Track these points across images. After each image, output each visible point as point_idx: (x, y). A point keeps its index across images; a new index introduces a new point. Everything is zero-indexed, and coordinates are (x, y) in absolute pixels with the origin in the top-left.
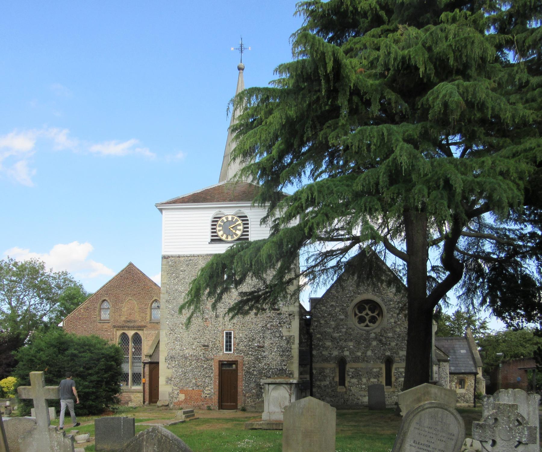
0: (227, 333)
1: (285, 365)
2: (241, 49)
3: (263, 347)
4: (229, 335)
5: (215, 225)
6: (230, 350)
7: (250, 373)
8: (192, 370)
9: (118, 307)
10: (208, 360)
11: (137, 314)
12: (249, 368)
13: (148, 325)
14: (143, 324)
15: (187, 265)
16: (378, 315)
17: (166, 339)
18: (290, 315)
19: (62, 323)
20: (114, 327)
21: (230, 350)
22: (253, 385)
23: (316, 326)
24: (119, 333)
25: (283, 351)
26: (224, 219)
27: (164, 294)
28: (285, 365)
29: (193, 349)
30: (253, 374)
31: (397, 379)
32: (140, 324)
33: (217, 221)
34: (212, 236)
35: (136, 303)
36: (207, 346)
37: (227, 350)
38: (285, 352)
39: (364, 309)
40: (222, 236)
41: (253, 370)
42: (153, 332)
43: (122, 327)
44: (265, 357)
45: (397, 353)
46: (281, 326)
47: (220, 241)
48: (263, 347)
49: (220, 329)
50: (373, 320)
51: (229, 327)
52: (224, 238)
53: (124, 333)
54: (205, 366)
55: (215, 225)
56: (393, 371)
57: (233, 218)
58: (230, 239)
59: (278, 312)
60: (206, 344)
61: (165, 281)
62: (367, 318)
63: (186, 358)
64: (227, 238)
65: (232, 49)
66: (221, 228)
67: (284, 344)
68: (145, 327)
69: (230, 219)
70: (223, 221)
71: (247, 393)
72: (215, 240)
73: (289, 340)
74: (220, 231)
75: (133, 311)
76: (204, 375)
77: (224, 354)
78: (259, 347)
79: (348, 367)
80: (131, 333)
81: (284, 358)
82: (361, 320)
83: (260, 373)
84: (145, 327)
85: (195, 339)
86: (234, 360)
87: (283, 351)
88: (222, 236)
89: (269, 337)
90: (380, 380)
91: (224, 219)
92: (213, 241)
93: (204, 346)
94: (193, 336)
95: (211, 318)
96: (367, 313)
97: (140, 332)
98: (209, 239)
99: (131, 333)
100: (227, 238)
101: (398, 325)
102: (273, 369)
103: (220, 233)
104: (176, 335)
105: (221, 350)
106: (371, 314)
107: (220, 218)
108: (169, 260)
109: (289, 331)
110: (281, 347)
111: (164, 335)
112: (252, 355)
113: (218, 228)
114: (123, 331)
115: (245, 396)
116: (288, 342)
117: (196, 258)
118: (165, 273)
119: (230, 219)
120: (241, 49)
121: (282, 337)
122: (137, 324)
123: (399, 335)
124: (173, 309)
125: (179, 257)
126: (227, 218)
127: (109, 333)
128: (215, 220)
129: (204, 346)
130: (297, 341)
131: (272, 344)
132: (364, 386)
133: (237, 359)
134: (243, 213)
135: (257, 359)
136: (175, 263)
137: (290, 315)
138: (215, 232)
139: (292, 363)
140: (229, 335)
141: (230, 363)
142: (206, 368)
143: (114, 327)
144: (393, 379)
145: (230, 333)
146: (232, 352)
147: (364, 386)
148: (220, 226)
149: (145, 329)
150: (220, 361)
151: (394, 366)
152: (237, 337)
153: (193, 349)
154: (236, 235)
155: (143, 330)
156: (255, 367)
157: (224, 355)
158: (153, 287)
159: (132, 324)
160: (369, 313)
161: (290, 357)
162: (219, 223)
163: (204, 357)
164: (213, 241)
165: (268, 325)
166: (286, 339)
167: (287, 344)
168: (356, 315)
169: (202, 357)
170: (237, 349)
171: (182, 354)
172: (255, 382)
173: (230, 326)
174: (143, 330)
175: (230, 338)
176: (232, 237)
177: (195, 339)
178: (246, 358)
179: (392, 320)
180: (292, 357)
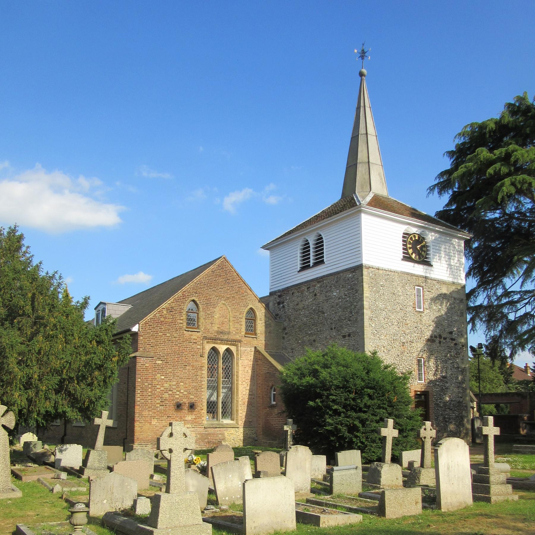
1: (461, 397)
2: (363, 55)
9: (209, 312)
12: (437, 400)
13: (244, 339)
14: (238, 337)
19: (137, 326)
20: (205, 338)
22: (441, 418)
24: (208, 347)
27: (367, 309)
28: (461, 397)
37: (419, 380)
40: (412, 254)
42: (249, 349)
43: (214, 340)
44: (447, 388)
46: (458, 357)
52: (413, 256)
53: (214, 349)
59: (454, 342)
65: (356, 51)
66: (411, 246)
68: (240, 341)
72: (407, 258)
74: (410, 248)
75: (226, 320)
80: (222, 348)
84: (240, 341)
97: (233, 348)
98: (401, 255)
99: (222, 348)
102: (454, 401)
103: (410, 251)
113: (408, 246)
114: (213, 345)
117: (393, 273)
120: (363, 55)
121: (458, 368)
122: (231, 337)
126: (415, 236)
127: (198, 347)
128: (406, 235)
136: (375, 275)
143: (205, 338)
146: (423, 382)
154: (423, 256)
156: (441, 399)
159: (225, 337)
166: (461, 371)
172: (442, 415)
174: (236, 345)
176: (420, 258)
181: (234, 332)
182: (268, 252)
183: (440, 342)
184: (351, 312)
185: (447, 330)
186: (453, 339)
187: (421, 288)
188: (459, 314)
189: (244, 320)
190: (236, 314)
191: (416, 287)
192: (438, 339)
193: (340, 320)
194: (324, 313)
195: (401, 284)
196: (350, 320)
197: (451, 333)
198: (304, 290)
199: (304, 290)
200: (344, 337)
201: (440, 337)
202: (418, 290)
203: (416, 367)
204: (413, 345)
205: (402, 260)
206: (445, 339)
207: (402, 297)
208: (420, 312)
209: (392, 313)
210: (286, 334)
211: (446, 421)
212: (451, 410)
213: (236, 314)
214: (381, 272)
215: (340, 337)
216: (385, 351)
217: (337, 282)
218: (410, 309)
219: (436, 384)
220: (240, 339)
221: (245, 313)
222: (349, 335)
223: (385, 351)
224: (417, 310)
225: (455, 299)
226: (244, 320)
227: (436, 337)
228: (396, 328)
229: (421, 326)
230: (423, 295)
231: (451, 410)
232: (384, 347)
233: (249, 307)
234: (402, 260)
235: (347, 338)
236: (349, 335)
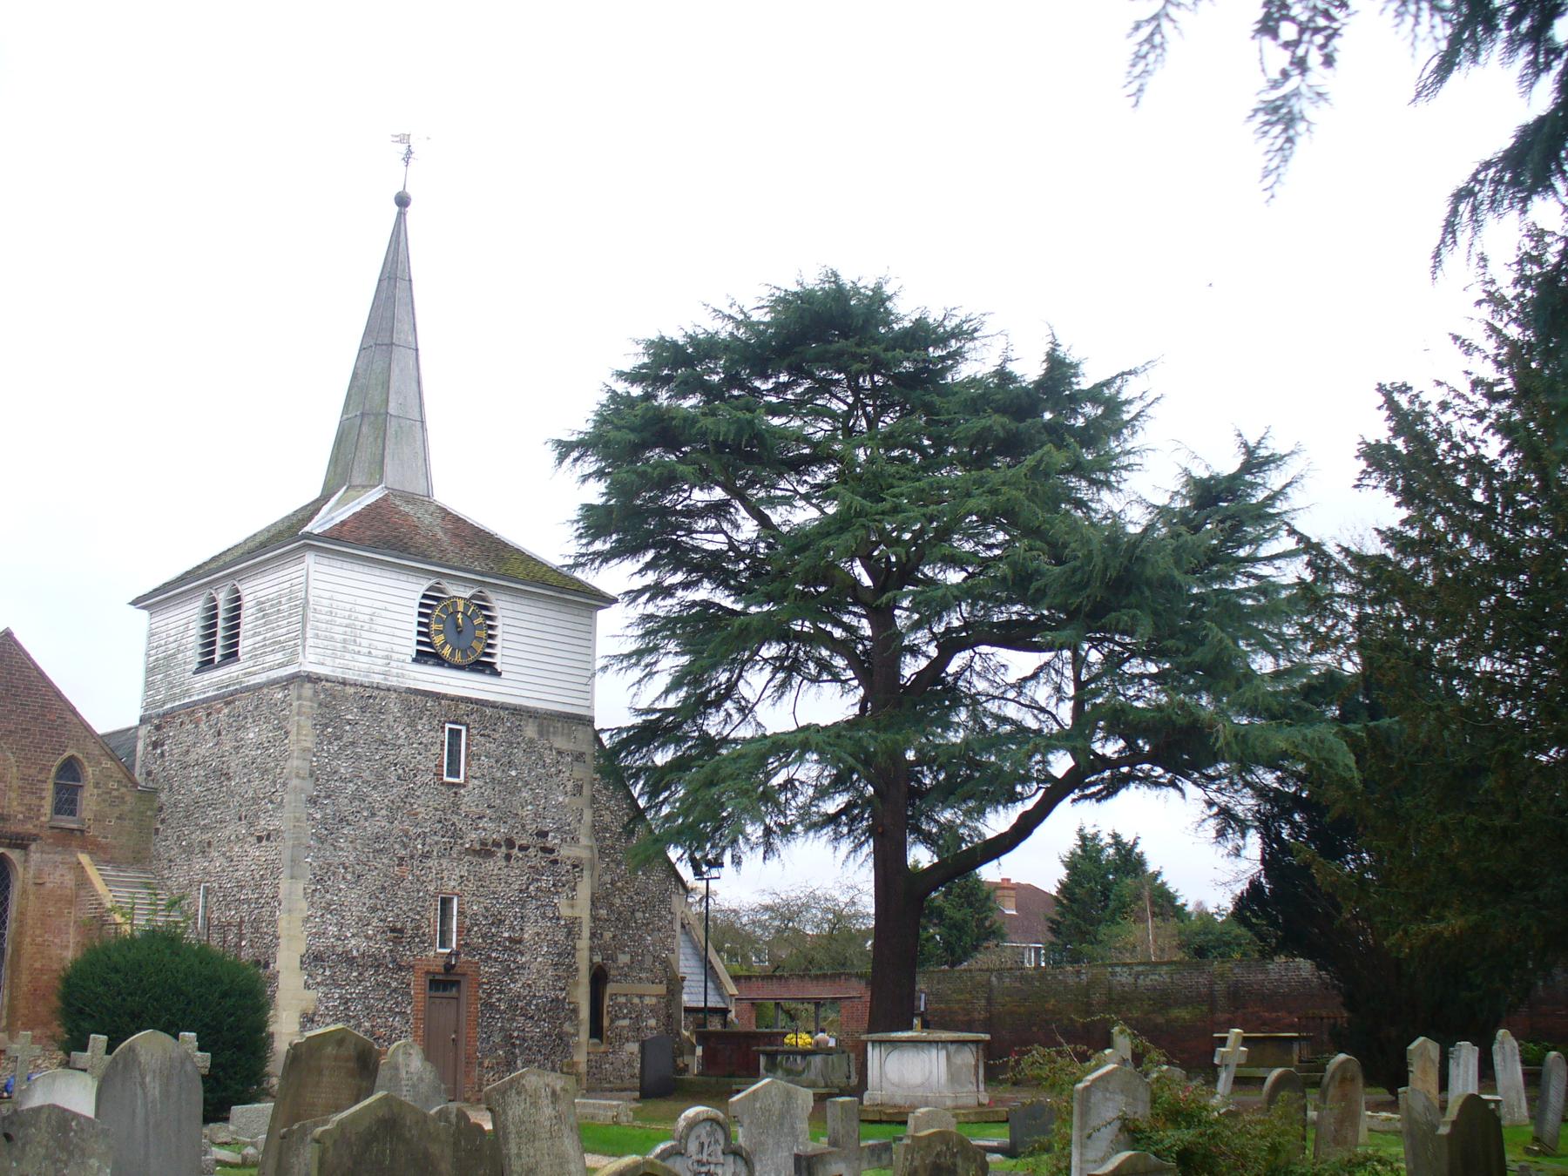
1: (562, 989)
7: (492, 1005)
8: (364, 996)
10: (400, 968)
11: (13, 795)
12: (490, 995)
14: (29, 827)
15: (363, 710)
17: (304, 905)
18: (575, 866)
22: (497, 1039)
25: (559, 955)
29: (367, 937)
30: (498, 1011)
31: (612, 1021)
32: (19, 829)
34: (419, 643)
35: (13, 760)
36: (401, 931)
37: (443, 945)
38: (563, 959)
41: (499, 1000)
44: (521, 967)
45: (615, 960)
47: (437, 659)
48: (520, 941)
52: (447, 651)
54: (394, 984)
56: (607, 1002)
58: (458, 658)
59: (552, 857)
60: (399, 925)
61: (309, 745)
63: (351, 961)
67: (561, 937)
68: (35, 838)
71: (485, 1056)
73: (571, 928)
74: (439, 632)
76: (390, 1009)
77: (437, 955)
78: (510, 939)
83: (512, 1007)
84: (35, 838)
85: (373, 909)
87: (559, 955)
89: (533, 918)
92: (421, 657)
93: (393, 930)
95: (412, 857)
98: (412, 649)
100: (452, 654)
101: (619, 889)
103: (439, 640)
104: (328, 896)
105: (431, 945)
108: (319, 687)
109: (572, 906)
110: (556, 943)
111: (301, 892)
112: (496, 959)
113: (434, 626)
115: (481, 1064)
116: (569, 933)
118: (310, 723)
123: (620, 914)
125: (344, 683)
129: (393, 930)
130: (586, 933)
131: (538, 934)
139: (577, 984)
140: (446, 903)
142: (395, 990)
144: (606, 1023)
149: (33, 847)
151: (611, 988)
152: (469, 912)
153: (367, 937)
155: (24, 847)
156: (501, 992)
158: (69, 716)
161: (572, 970)
163: (394, 961)
164: (421, 657)
169: (389, 959)
171: (340, 950)
172: (502, 1029)
173: (453, 883)
174: (24, 847)
177: (373, 909)
178: (484, 969)
179: (608, 878)
180: (577, 970)
181: (20, 816)
182: (145, 613)
183: (508, 857)
184: (274, 783)
185: (532, 828)
186: (545, 850)
187: (464, 729)
188: (569, 788)
189: (50, 786)
190: (32, 771)
191: (448, 726)
192: (504, 849)
193: (255, 800)
194: (229, 779)
195: (406, 720)
196: (271, 802)
197: (543, 834)
198: (200, 719)
199: (200, 719)
200: (260, 839)
201: (510, 843)
202: (455, 734)
203: (434, 915)
204: (430, 863)
205: (414, 660)
206: (523, 848)
207: (404, 751)
208: (453, 784)
209: (374, 788)
210: (163, 821)
211: (513, 1045)
212: (532, 1018)
213: (32, 771)
215: (253, 840)
216: (349, 877)
217: (257, 707)
218: (428, 778)
219: (489, 957)
220: (35, 831)
221: (54, 770)
222: (268, 836)
223: (349, 877)
224: (446, 779)
225: (559, 753)
226: (51, 786)
227: (497, 844)
229: (455, 819)
230: (468, 745)
231: (532, 1018)
232: (345, 868)
233: (66, 755)
234: (414, 660)
235: (264, 843)
236: (268, 836)
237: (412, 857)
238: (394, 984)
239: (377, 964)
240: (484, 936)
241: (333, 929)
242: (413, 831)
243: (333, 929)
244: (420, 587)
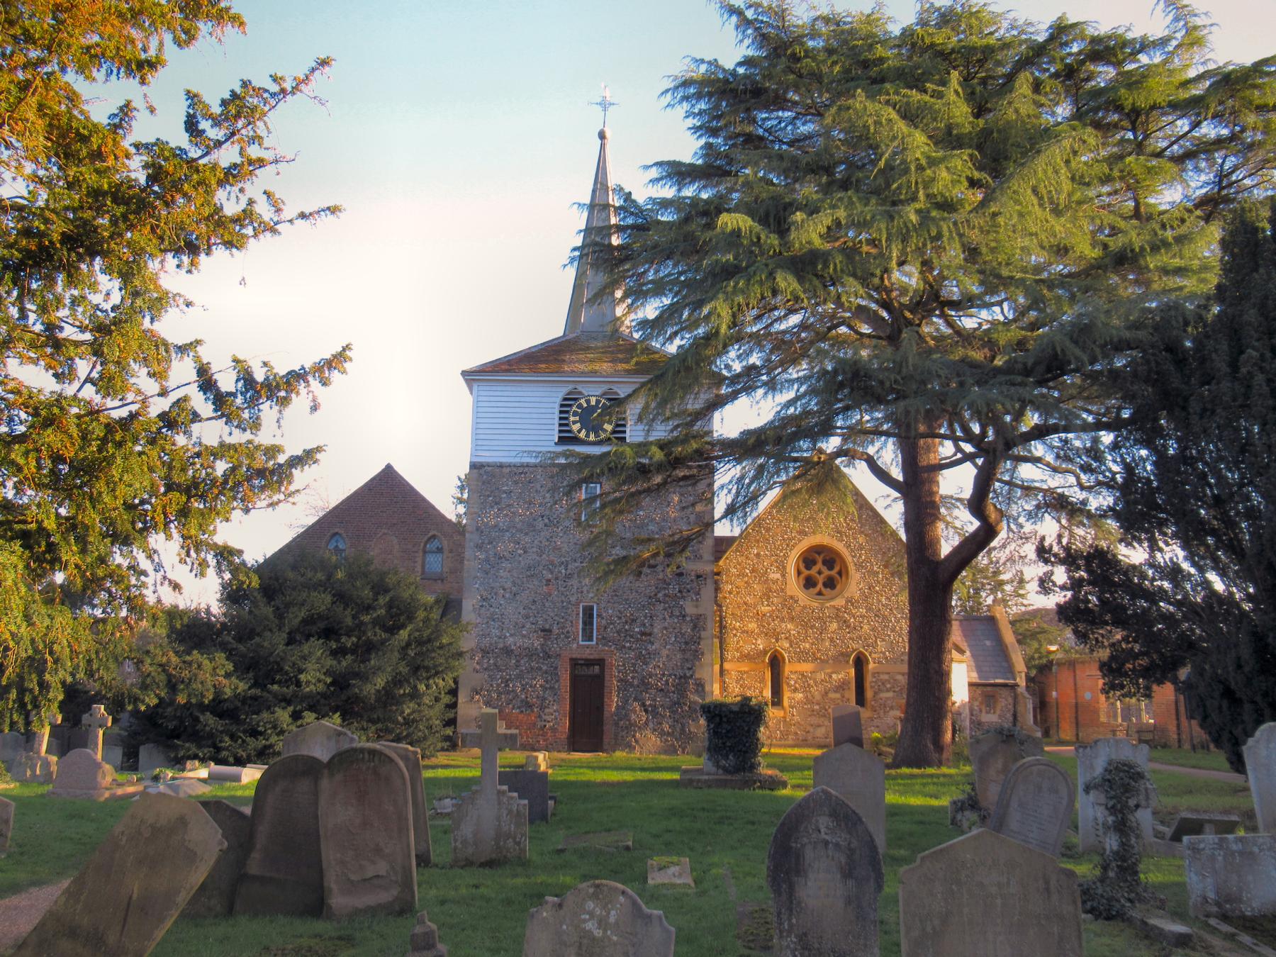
0: (585, 609)
3: (650, 634)
4: (588, 612)
5: (567, 412)
6: (591, 639)
7: (627, 681)
15: (516, 483)
16: (840, 573)
21: (591, 639)
23: (730, 593)
25: (686, 643)
26: (583, 401)
29: (524, 636)
30: (632, 685)
33: (570, 406)
39: (814, 563)
40: (579, 431)
46: (683, 597)
47: (575, 440)
48: (650, 634)
49: (573, 599)
50: (830, 584)
51: (589, 598)
52: (582, 435)
54: (544, 668)
55: (567, 412)
57: (598, 402)
58: (592, 438)
60: (547, 627)
62: (821, 579)
64: (588, 436)
67: (687, 629)
69: (593, 403)
70: (580, 406)
74: (574, 423)
78: (643, 634)
79: (788, 669)
81: (688, 655)
82: (809, 583)
85: (527, 617)
86: (597, 657)
88: (579, 431)
90: (847, 695)
91: (583, 401)
94: (523, 612)
95: (557, 578)
96: (820, 571)
100: (588, 436)
103: (576, 427)
106: (826, 572)
107: (575, 399)
108: (482, 471)
110: (683, 635)
112: (630, 648)
113: (572, 419)
115: (616, 724)
116: (695, 627)
119: (593, 403)
124: (487, 560)
126: (588, 402)
128: (567, 403)
131: (666, 628)
132: (816, 707)
133: (602, 656)
134: (616, 393)
135: (639, 656)
137: (698, 577)
138: (567, 425)
140: (588, 612)
141: (589, 663)
142: (546, 672)
144: (869, 694)
145: (591, 608)
147: (816, 707)
148: (575, 414)
150: (571, 659)
156: (635, 671)
157: (581, 647)
160: (824, 569)
162: (574, 408)
165: (660, 595)
167: (693, 630)
168: (799, 573)
170: (604, 638)
171: (501, 645)
175: (591, 616)
214: (506, 470)
228: (535, 556)
237: (557, 578)
238: (544, 668)
239: (530, 654)
240: (618, 632)
241: (495, 632)
242: (557, 561)
243: (495, 632)
244: (558, 394)
